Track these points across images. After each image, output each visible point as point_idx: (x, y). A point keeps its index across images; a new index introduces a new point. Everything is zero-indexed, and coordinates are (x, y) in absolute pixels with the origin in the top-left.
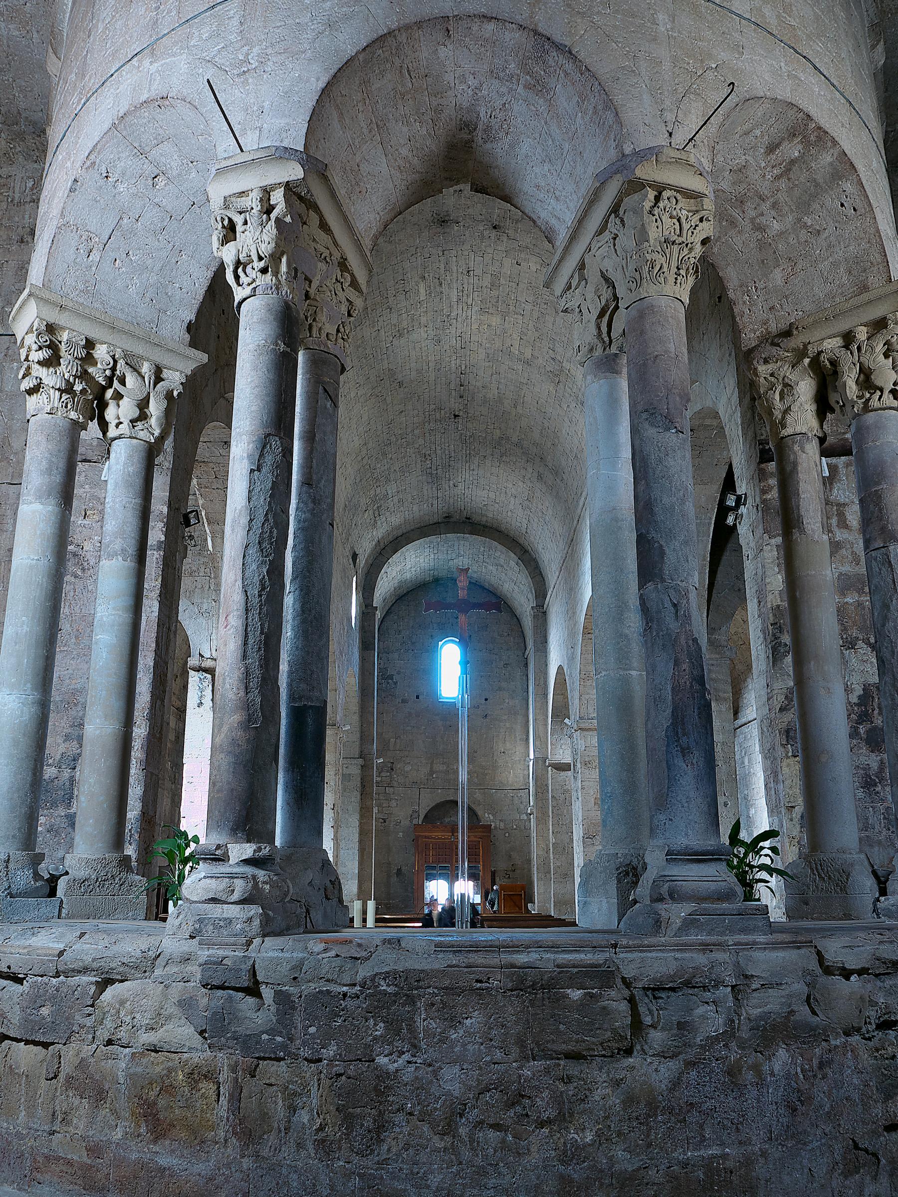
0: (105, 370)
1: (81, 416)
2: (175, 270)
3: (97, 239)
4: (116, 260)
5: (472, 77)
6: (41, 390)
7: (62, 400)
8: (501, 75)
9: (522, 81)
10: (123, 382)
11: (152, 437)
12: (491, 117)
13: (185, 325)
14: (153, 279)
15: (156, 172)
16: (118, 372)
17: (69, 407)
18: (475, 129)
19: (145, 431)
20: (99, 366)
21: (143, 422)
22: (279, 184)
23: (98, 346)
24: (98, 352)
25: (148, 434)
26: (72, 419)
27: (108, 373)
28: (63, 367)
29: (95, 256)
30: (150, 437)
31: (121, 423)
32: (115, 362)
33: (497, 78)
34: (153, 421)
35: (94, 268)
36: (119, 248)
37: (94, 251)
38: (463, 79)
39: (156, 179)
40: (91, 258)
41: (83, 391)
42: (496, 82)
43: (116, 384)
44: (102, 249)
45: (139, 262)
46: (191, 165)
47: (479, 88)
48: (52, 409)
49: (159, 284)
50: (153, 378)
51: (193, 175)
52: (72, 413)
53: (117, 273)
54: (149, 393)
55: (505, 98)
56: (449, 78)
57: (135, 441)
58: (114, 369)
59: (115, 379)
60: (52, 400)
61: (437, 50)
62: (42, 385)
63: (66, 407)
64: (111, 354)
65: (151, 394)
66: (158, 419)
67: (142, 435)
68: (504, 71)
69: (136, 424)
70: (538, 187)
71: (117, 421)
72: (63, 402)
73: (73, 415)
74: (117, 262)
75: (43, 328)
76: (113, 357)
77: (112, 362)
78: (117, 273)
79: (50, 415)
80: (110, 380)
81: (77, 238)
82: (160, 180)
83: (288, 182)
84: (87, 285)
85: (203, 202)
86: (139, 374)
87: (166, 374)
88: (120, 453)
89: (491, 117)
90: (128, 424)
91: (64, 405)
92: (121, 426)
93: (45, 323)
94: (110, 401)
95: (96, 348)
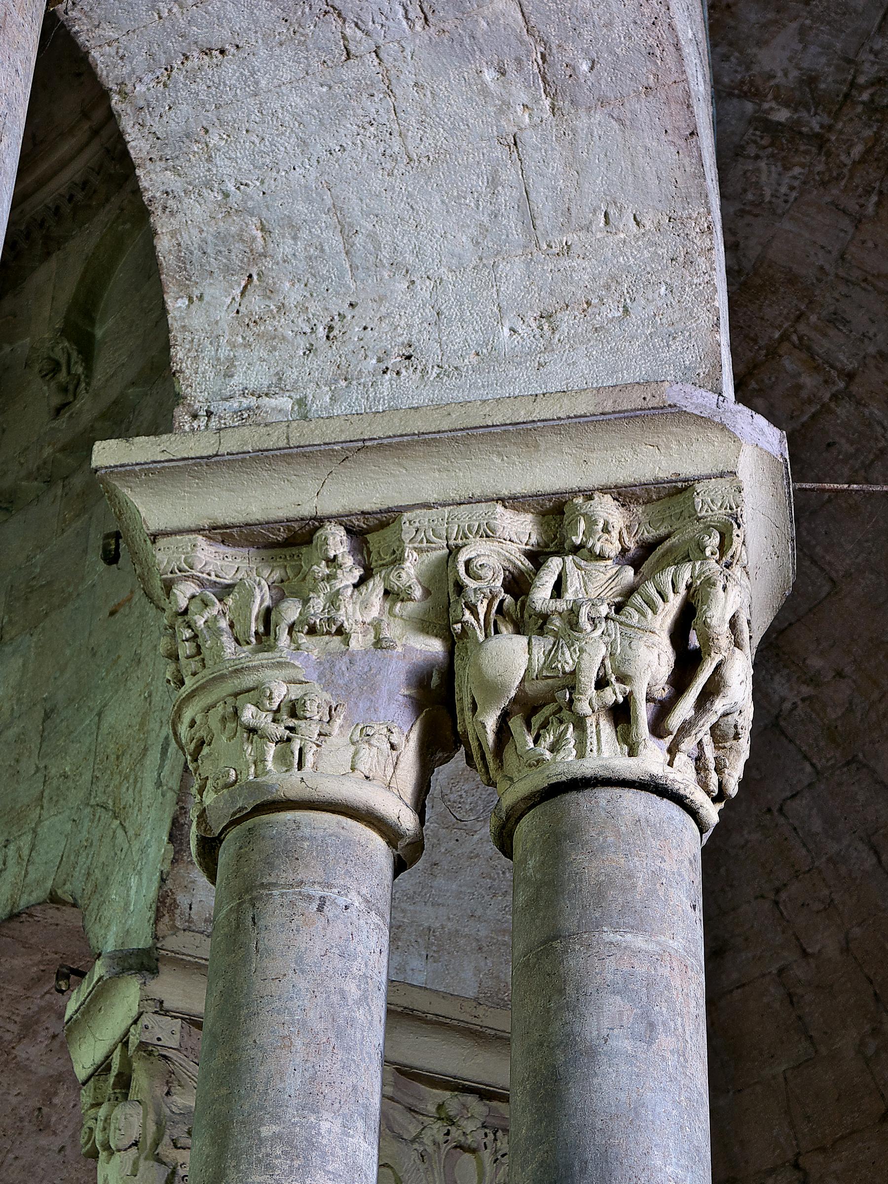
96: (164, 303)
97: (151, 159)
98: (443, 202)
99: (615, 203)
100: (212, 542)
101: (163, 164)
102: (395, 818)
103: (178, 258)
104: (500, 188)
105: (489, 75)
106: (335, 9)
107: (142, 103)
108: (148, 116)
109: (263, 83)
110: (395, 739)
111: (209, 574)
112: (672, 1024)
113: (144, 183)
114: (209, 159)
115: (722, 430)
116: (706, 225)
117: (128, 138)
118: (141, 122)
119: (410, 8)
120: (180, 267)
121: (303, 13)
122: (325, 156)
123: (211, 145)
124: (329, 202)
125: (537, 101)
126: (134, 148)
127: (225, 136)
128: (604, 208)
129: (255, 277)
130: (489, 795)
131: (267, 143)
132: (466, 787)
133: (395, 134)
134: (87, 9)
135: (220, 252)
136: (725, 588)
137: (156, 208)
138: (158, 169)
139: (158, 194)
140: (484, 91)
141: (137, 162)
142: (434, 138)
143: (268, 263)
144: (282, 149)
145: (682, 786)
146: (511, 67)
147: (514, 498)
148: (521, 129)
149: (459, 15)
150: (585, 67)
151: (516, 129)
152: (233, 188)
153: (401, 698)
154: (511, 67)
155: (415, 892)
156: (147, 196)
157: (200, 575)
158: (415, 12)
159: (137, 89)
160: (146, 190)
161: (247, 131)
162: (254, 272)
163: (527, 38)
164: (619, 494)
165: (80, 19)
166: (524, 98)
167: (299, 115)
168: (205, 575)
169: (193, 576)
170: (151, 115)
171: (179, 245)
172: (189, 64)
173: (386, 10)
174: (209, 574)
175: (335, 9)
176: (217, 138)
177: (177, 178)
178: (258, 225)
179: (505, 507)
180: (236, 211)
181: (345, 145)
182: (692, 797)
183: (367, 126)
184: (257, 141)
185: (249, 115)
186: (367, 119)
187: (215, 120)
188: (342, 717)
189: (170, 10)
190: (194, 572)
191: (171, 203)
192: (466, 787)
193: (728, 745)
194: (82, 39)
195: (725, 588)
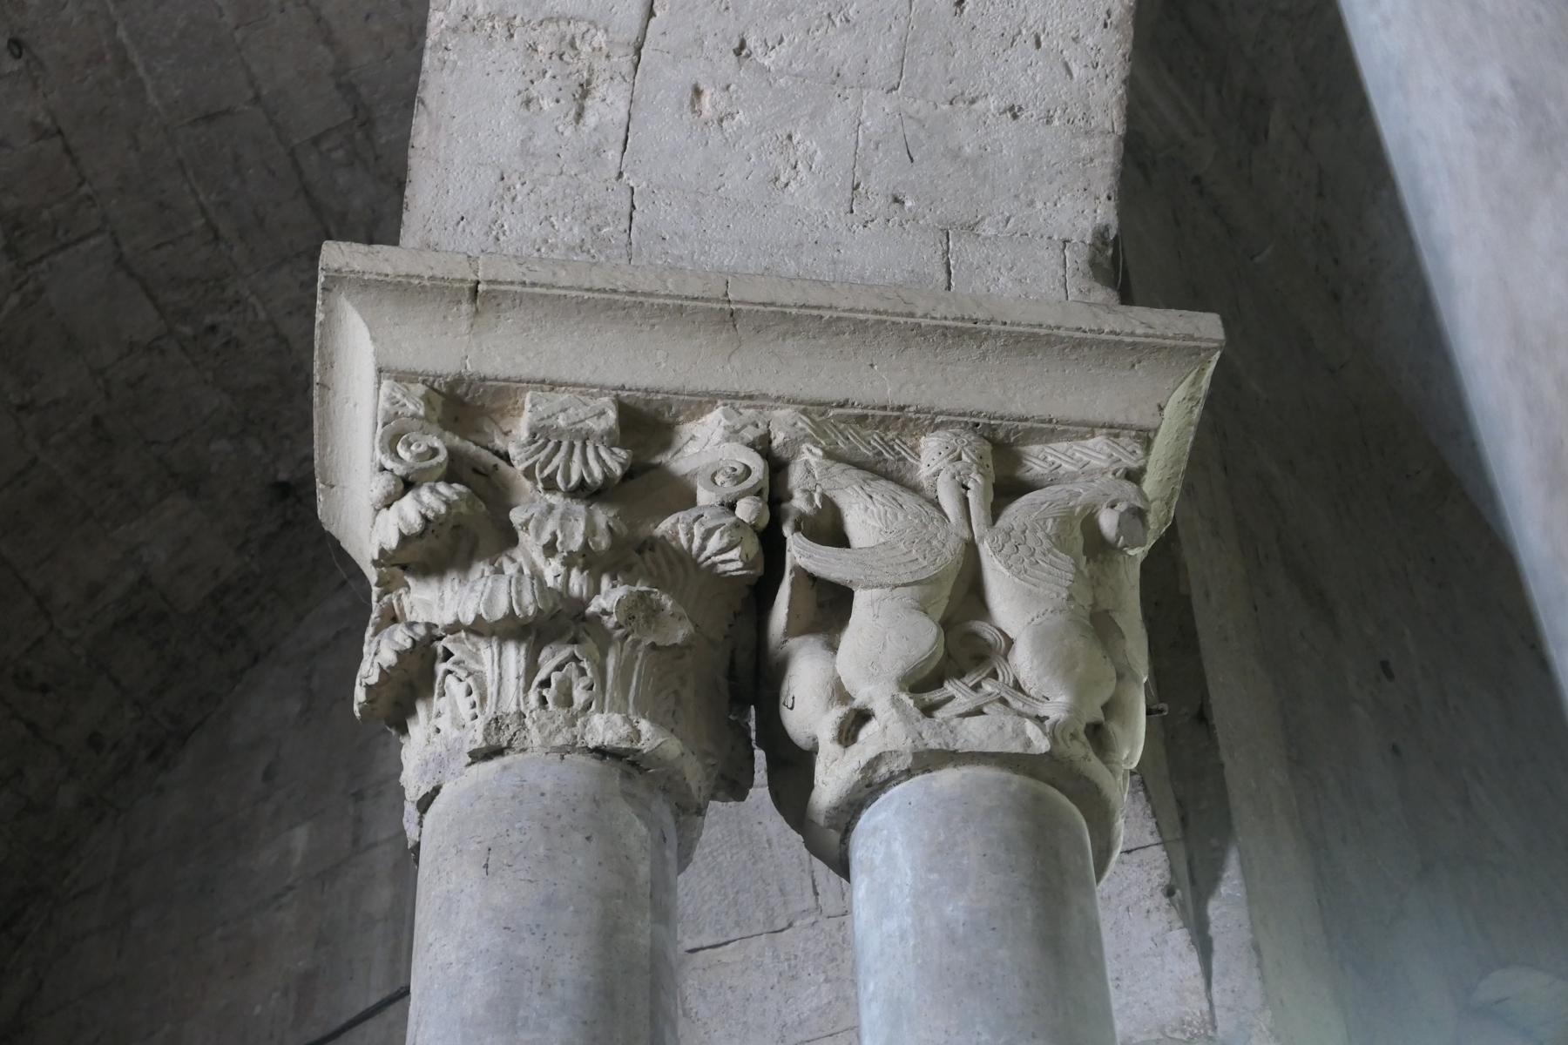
0: (732, 507)
1: (644, 726)
2: (960, 43)
3: (600, 38)
4: (697, 92)
6: (441, 668)
7: (541, 676)
10: (829, 529)
11: (1031, 729)
13: (1078, 257)
14: (877, 112)
16: (799, 503)
17: (579, 696)
19: (993, 710)
20: (704, 496)
21: (971, 680)
23: (687, 429)
24: (692, 449)
25: (1010, 722)
26: (601, 752)
27: (746, 510)
28: (530, 545)
29: (607, 106)
30: (1019, 732)
31: (862, 717)
32: (777, 467)
34: (1024, 662)
35: (613, 154)
36: (699, 41)
37: (600, 90)
40: (591, 119)
41: (640, 611)
43: (799, 552)
44: (626, 67)
45: (798, 67)
48: (497, 723)
49: (912, 126)
50: (975, 482)
52: (597, 720)
53: (715, 137)
54: (971, 549)
57: (948, 778)
58: (775, 494)
59: (787, 530)
60: (492, 690)
62: (439, 646)
63: (566, 700)
64: (750, 434)
65: (985, 549)
66: (1042, 638)
67: (975, 734)
69: (936, 695)
71: (838, 712)
72: (546, 683)
73: (604, 728)
74: (706, 100)
75: (415, 406)
76: (763, 446)
77: (757, 465)
78: (715, 137)
79: (494, 764)
80: (771, 543)
81: (514, 60)
84: (596, 219)
86: (915, 489)
87: (1038, 459)
88: (890, 858)
90: (895, 702)
91: (549, 694)
92: (868, 731)
93: (420, 389)
94: (793, 642)
95: (678, 443)
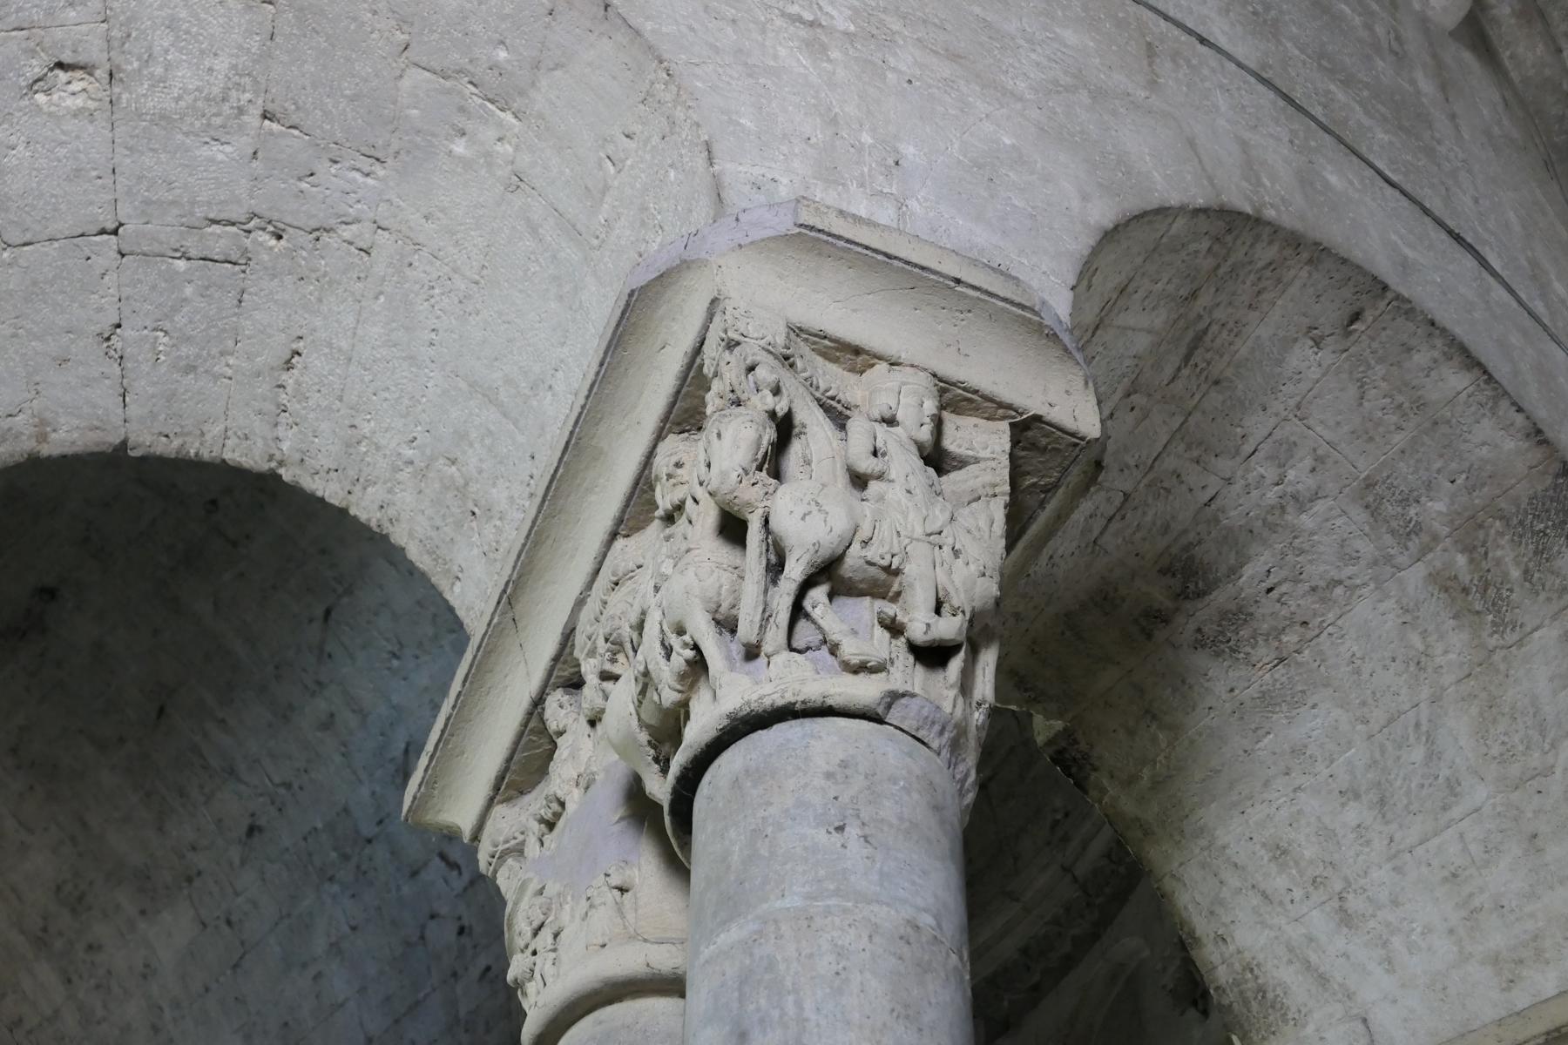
5: (1308, 462)
8: (1390, 509)
9: (1436, 559)
12: (1270, 590)
15: (93, 51)
18: (1200, 595)
22: (1001, 405)
33: (1373, 510)
38: (1283, 454)
39: (62, 76)
42: (1359, 515)
46: (252, 119)
47: (1301, 502)
51: (219, 152)
55: (1350, 570)
56: (1257, 425)
61: (1296, 340)
68: (1405, 502)
70: (1280, 853)
82: (77, 86)
83: (1037, 419)
85: (156, 248)
89: (1270, 590)
96: (446, 601)
97: (349, 493)
98: (520, 291)
99: (606, 140)
100: (514, 801)
101: (358, 488)
102: (648, 970)
103: (428, 552)
104: (540, 230)
105: (459, 147)
106: (318, 230)
107: (297, 456)
108: (313, 462)
109: (344, 345)
110: (616, 880)
111: (515, 838)
112: (776, 1014)
113: (363, 517)
114: (378, 448)
115: (688, 268)
116: (665, 76)
117: (319, 494)
118: (313, 471)
119: (358, 166)
120: (435, 560)
121: (304, 259)
122: (431, 351)
123: (368, 435)
124: (463, 385)
125: (500, 124)
126: (330, 496)
127: (369, 417)
128: (604, 156)
129: (476, 510)
130: (1535, 716)
131: (393, 388)
132: (1501, 729)
133: (451, 275)
134: (178, 430)
135: (444, 515)
136: (719, 435)
137: (388, 528)
138: (360, 494)
139: (379, 515)
140: (467, 164)
141: (343, 505)
142: (474, 245)
143: (473, 487)
144: (405, 381)
145: (775, 696)
146: (461, 121)
147: (619, 521)
148: (513, 163)
149: (391, 127)
150: (502, 54)
151: (510, 167)
152: (411, 452)
153: (617, 828)
154: (461, 121)
155: (1531, 886)
156: (373, 524)
157: (507, 846)
158: (365, 164)
159: (284, 449)
160: (369, 520)
161: (375, 394)
162: (471, 506)
163: (448, 84)
164: (679, 424)
165: (185, 443)
166: (491, 134)
167: (389, 341)
168: (513, 842)
169: (502, 852)
170: (313, 458)
171: (421, 541)
172: (289, 389)
173: (348, 187)
174: (515, 838)
175: (318, 230)
176: (366, 424)
177: (377, 487)
178: (447, 462)
179: (628, 536)
180: (427, 467)
181: (433, 327)
182: (800, 698)
183: (431, 292)
184: (387, 395)
185: (362, 381)
186: (426, 287)
187: (349, 411)
188: (569, 898)
189: (228, 365)
190: (501, 848)
191: (391, 512)
192: (1501, 729)
193: (895, 588)
194: (206, 455)
195: (719, 435)
